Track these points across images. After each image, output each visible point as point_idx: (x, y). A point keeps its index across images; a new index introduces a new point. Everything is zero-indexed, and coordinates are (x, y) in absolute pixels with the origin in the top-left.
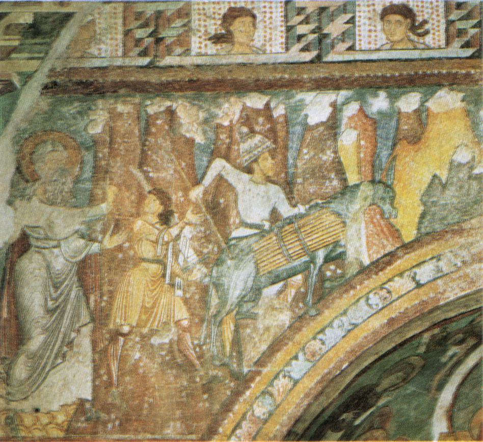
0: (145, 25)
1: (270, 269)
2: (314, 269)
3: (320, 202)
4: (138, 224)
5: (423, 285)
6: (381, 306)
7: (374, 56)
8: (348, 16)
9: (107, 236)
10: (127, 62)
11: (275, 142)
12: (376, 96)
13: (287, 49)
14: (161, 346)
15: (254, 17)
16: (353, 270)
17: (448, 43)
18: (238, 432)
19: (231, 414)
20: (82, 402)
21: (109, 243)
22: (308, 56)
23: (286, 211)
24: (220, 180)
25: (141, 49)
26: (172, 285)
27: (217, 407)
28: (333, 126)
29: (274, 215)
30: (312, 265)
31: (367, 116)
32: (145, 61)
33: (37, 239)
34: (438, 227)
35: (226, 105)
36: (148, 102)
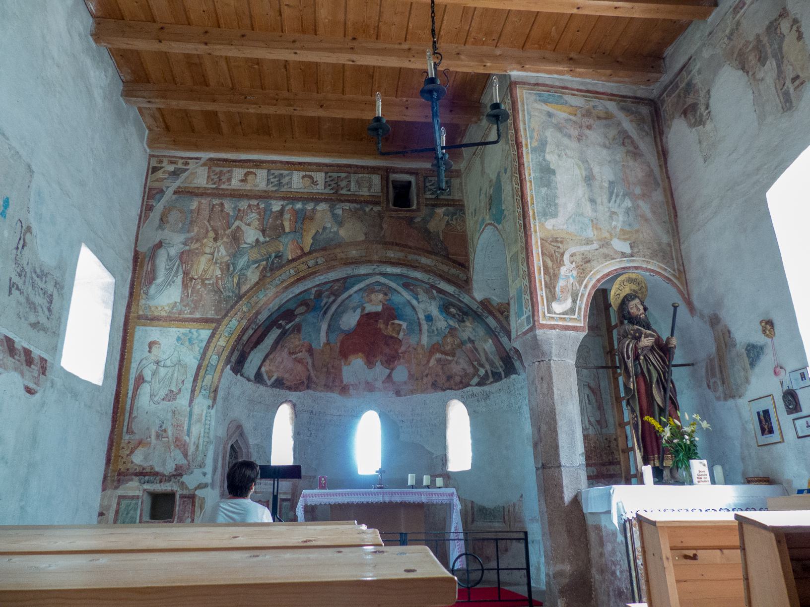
4: (205, 240)
7: (298, 191)
10: (207, 186)
14: (209, 284)
20: (176, 303)
21: (194, 246)
22: (274, 189)
23: (262, 239)
24: (238, 227)
26: (216, 263)
27: (229, 307)
28: (281, 212)
29: (257, 241)
32: (214, 186)
33: (165, 243)
34: (317, 248)
35: (243, 203)
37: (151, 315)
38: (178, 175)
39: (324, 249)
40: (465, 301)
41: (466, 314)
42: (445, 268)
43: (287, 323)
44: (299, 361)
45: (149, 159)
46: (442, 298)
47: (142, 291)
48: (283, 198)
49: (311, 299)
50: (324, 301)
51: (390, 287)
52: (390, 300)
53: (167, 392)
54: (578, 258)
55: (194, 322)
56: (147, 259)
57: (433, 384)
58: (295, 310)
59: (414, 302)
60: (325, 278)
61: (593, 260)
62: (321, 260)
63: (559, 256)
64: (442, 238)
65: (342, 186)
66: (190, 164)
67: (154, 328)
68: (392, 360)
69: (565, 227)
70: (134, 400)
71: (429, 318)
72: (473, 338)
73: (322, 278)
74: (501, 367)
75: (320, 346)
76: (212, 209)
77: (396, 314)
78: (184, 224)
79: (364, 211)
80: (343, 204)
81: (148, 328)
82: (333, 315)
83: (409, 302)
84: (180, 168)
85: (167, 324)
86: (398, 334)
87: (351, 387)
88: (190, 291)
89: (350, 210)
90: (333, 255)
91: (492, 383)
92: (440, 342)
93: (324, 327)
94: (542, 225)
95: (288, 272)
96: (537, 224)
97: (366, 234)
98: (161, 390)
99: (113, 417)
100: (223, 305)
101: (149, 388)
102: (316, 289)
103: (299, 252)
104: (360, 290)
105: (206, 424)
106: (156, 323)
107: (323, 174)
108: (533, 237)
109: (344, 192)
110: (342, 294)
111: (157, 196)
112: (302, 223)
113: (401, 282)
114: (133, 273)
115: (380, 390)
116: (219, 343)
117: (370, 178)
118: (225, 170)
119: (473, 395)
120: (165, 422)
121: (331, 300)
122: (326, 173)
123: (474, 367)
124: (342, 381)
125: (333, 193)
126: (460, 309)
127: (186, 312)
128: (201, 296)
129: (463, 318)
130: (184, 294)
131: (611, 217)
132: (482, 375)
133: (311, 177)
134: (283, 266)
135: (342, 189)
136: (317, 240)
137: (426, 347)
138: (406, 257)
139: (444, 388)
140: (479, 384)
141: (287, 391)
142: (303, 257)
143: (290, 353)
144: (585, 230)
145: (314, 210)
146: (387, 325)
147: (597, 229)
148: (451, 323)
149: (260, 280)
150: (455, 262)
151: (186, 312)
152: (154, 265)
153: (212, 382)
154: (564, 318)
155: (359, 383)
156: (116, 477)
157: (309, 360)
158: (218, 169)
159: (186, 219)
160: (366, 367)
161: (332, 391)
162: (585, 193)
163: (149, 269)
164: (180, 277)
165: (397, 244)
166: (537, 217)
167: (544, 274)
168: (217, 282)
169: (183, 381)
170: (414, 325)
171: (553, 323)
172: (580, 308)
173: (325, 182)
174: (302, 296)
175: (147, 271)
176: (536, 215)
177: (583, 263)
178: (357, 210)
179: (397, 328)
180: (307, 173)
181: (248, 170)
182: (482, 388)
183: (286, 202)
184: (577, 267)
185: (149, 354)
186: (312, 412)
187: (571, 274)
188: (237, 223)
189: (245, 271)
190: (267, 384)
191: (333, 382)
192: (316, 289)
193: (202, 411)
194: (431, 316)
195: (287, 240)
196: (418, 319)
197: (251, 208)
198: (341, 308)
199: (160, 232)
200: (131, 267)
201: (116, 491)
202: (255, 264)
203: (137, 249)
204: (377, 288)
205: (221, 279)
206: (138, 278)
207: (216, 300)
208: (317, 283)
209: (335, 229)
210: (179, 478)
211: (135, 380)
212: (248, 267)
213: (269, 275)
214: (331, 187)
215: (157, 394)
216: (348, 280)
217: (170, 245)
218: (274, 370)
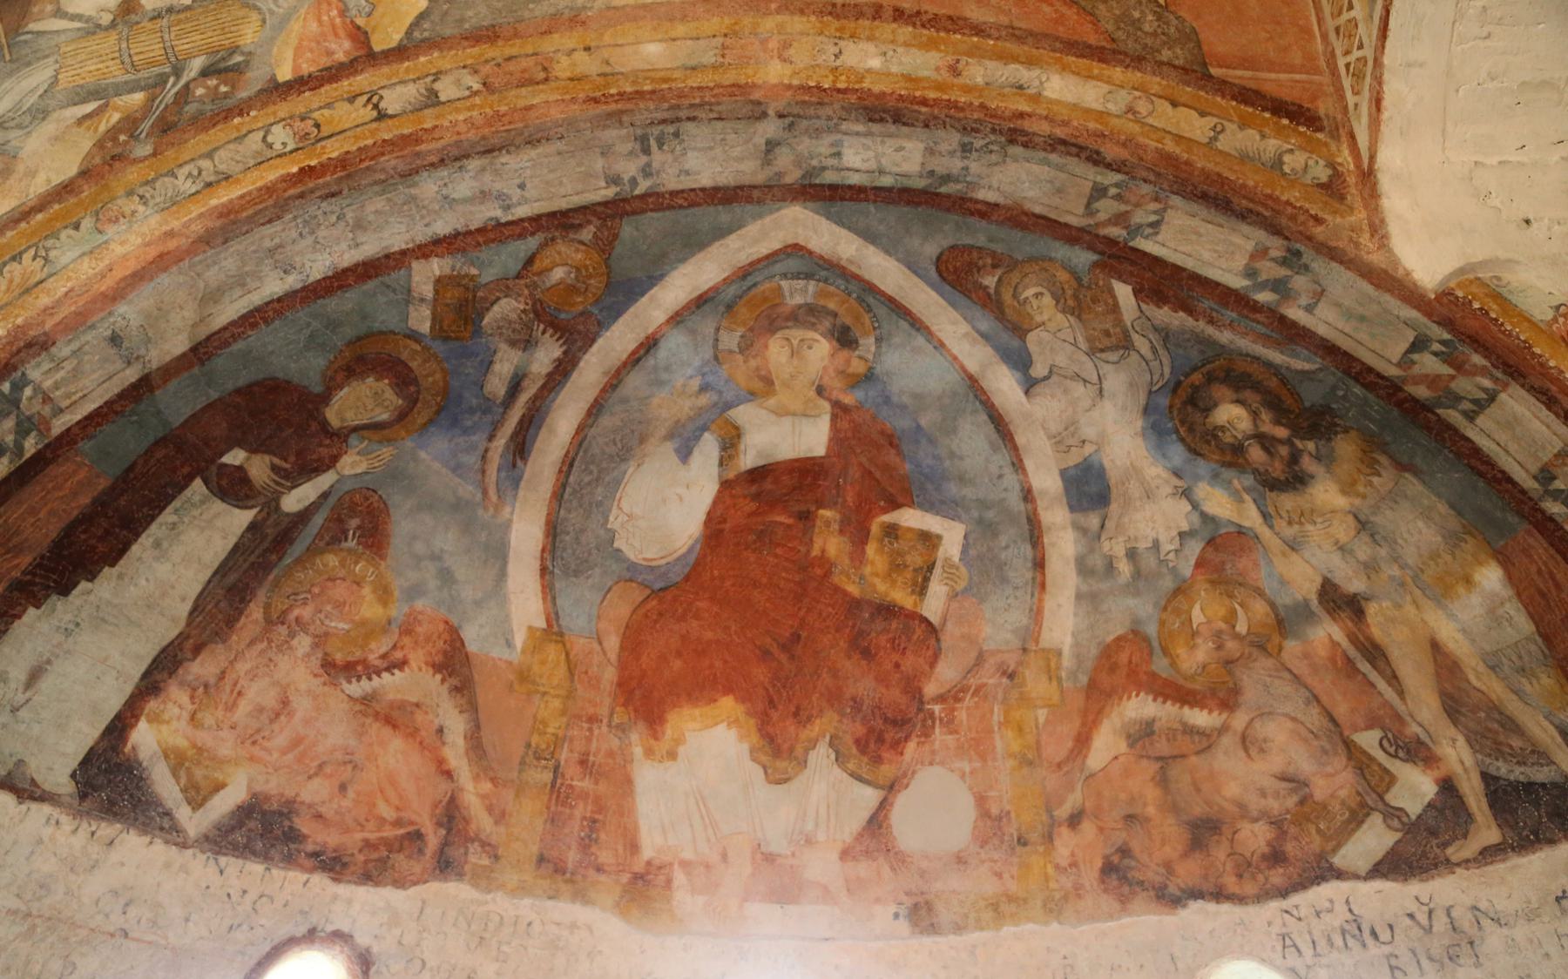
1: (82, 82)
2: (174, 85)
5: (392, 117)
6: (289, 148)
30: (172, 80)
34: (448, 32)
40: (1324, 321)
42: (1197, 127)
44: (395, 717)
46: (1165, 335)
49: (414, 336)
51: (871, 288)
52: (869, 377)
57: (1108, 869)
58: (325, 398)
59: (1004, 385)
62: (458, 82)
68: (890, 735)
75: (509, 644)
77: (908, 467)
82: (568, 464)
86: (921, 589)
87: (679, 878)
91: (1489, 854)
92: (1152, 630)
103: (342, 50)
104: (701, 302)
110: (602, 325)
113: (931, 250)
115: (826, 895)
123: (1359, 761)
124: (634, 847)
129: (1294, 458)
132: (1414, 809)
137: (1067, 661)
138: (954, 70)
140: (1392, 866)
141: (320, 881)
142: (356, 72)
143: (328, 665)
146: (860, 537)
148: (1219, 502)
149: (84, 174)
150: (1246, 96)
157: (456, 725)
161: (581, 896)
170: (1003, 540)
179: (915, 559)
182: (1415, 888)
191: (587, 844)
192: (437, 266)
194: (1101, 473)
196: (1028, 495)
198: (606, 421)
202: (84, 101)
204: (798, 293)
208: (442, 227)
212: (40, 114)
216: (627, 230)
218: (225, 751)
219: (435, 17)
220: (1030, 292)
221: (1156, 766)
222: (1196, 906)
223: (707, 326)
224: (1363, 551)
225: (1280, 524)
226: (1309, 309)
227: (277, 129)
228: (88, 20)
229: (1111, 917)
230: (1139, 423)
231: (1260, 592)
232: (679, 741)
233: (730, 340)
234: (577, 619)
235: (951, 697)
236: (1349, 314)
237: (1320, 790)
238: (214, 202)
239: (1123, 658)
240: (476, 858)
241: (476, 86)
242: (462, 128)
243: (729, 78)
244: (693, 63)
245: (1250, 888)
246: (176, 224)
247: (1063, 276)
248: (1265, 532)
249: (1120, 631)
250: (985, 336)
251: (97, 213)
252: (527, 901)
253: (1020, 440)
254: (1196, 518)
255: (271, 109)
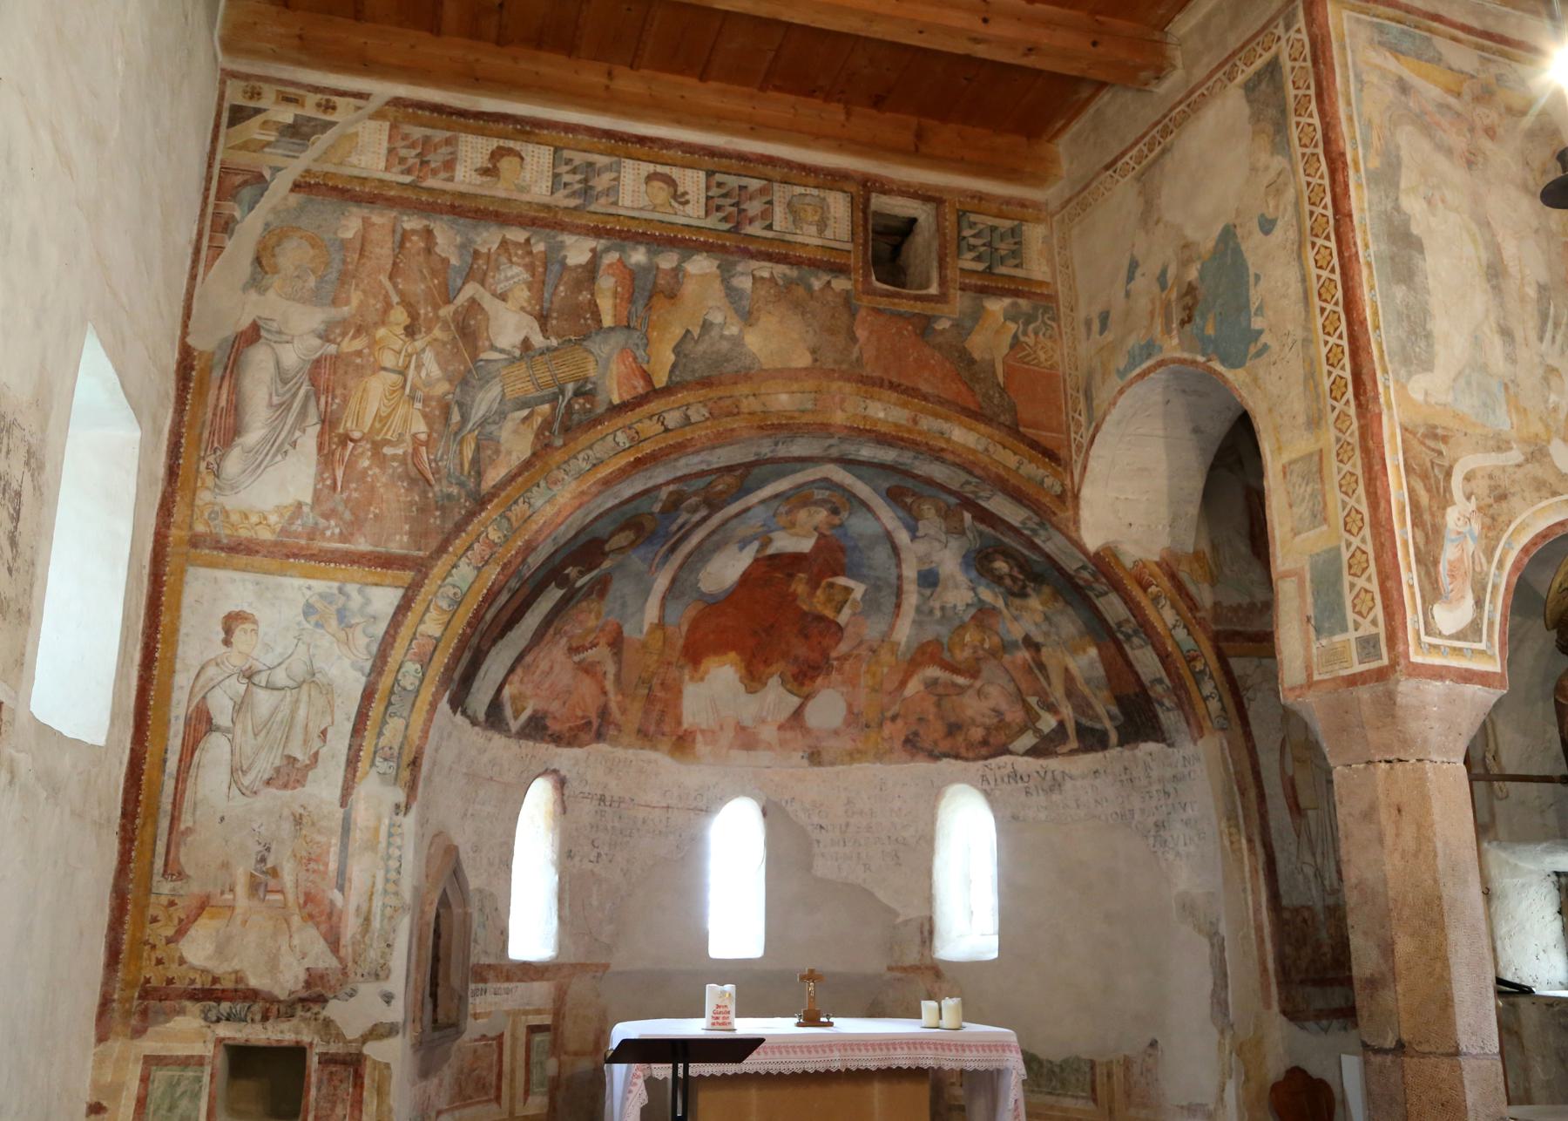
0: (413, 146)
3: (573, 338)
4: (381, 332)
8: (614, 175)
9: (347, 339)
10: (388, 177)
11: (533, 276)
12: (634, 249)
13: (552, 193)
14: (394, 457)
15: (522, 158)
16: (601, 409)
17: (707, 214)
18: (469, 553)
19: (463, 534)
20: (300, 505)
21: (349, 345)
22: (573, 202)
23: (538, 340)
25: (404, 167)
26: (412, 398)
27: (449, 525)
28: (591, 271)
29: (526, 344)
31: (625, 266)
32: (407, 179)
33: (268, 331)
34: (689, 378)
35: (485, 234)
36: (405, 218)
37: (227, 536)
38: (307, 137)
39: (706, 383)
40: (1049, 547)
41: (1037, 578)
42: (1011, 460)
43: (582, 574)
44: (587, 669)
45: (223, 83)
46: (981, 534)
47: (203, 465)
48: (597, 232)
49: (652, 514)
50: (680, 521)
51: (854, 496)
52: (841, 525)
53: (277, 763)
54: (1481, 486)
55: (353, 562)
56: (217, 373)
57: (907, 741)
58: (607, 541)
59: (903, 537)
60: (702, 462)
61: (1513, 494)
63: (1441, 477)
64: (1001, 380)
65: (751, 213)
66: (339, 110)
67: (237, 575)
69: (1450, 399)
70: (185, 781)
71: (929, 579)
72: (1039, 639)
73: (695, 459)
74: (1112, 718)
75: (641, 632)
76: (402, 245)
78: (321, 280)
79: (809, 288)
80: (754, 264)
81: (221, 574)
82: (690, 554)
83: (889, 536)
84: (310, 119)
85: (275, 564)
86: (839, 610)
87: (699, 738)
88: (339, 473)
89: (772, 279)
90: (728, 402)
91: (1072, 752)
92: (945, 640)
93: (662, 582)
94: (1402, 388)
95: (610, 438)
96: (1392, 384)
97: (813, 351)
98: (263, 754)
99: (123, 827)
100: (434, 520)
101: (227, 748)
102: (672, 488)
103: (640, 387)
104: (776, 496)
105: (389, 857)
106: (243, 559)
107: (702, 175)
108: (1385, 419)
109: (755, 229)
110: (729, 504)
111: (246, 193)
112: (648, 307)
113: (886, 485)
114: (176, 411)
115: (769, 747)
116: (422, 628)
117: (824, 199)
118: (439, 135)
119: (1015, 776)
120: (273, 847)
121: (697, 517)
122: (710, 174)
123: (1027, 708)
124: (679, 723)
125: (729, 231)
126: (1022, 564)
127: (328, 533)
128: (372, 489)
129: (1024, 587)
130: (323, 480)
131: (1546, 379)
132: (1046, 730)
133: (670, 182)
134: (598, 421)
135: (751, 221)
136: (686, 356)
138: (915, 422)
139: (936, 752)
140: (1033, 752)
141: (552, 747)
142: (649, 402)
144: (1494, 411)
145: (677, 271)
147: (1517, 410)
148: (987, 595)
149: (534, 454)
150: (1034, 445)
151: (328, 533)
152: (236, 390)
153: (405, 737)
154: (1461, 649)
155: (722, 728)
156: (136, 1003)
157: (611, 669)
158: (417, 132)
159: (327, 264)
160: (742, 688)
161: (654, 748)
162: (1487, 310)
163: (223, 403)
164: (314, 430)
165: (893, 387)
166: (1389, 366)
167: (1414, 525)
168: (416, 452)
169: (324, 733)
171: (1437, 660)
172: (1491, 624)
173: (708, 198)
174: (635, 503)
175: (216, 406)
176: (1386, 358)
177: (1491, 501)
178: (790, 283)
179: (839, 597)
180: (660, 169)
181: (502, 143)
182: (1042, 762)
183: (602, 241)
184: (1480, 509)
185: (224, 649)
186: (602, 799)
187: (1468, 528)
188: (471, 289)
189: (493, 427)
190: (509, 730)
191: (660, 722)
192: (672, 488)
193: (379, 819)
195: (606, 349)
196: (900, 577)
197: (507, 250)
198: (715, 538)
199: (253, 295)
200: (172, 393)
201: (137, 1042)
202: (521, 408)
203: (190, 340)
204: (820, 494)
205: (426, 444)
206: (191, 426)
207: (412, 503)
208: (679, 474)
209: (733, 330)
210: (316, 1008)
211: (187, 724)
212: (502, 415)
213: (559, 442)
214: (721, 215)
215: (250, 768)
216: (756, 471)
217: (282, 336)
218: (528, 693)
219: (680, 367)
220: (925, 507)
221: (935, 698)
222: (945, 760)
223: (775, 504)
224: (1045, 627)
225: (1013, 610)
226: (1044, 542)
227: (619, 433)
228: (508, 353)
229: (906, 762)
230: (960, 560)
231: (997, 634)
232: (706, 672)
233: (783, 509)
234: (671, 618)
235: (844, 658)
236: (1059, 549)
237: (1008, 718)
238: (599, 476)
239: (929, 650)
240: (612, 732)
241: (707, 415)
242: (704, 440)
243: (819, 419)
244: (802, 408)
245: (971, 755)
246: (584, 487)
247: (942, 504)
248: (1005, 611)
249: (930, 638)
250: (899, 518)
251: (545, 478)
252: (631, 751)
253: (902, 556)
254: (975, 599)
255: (614, 421)
